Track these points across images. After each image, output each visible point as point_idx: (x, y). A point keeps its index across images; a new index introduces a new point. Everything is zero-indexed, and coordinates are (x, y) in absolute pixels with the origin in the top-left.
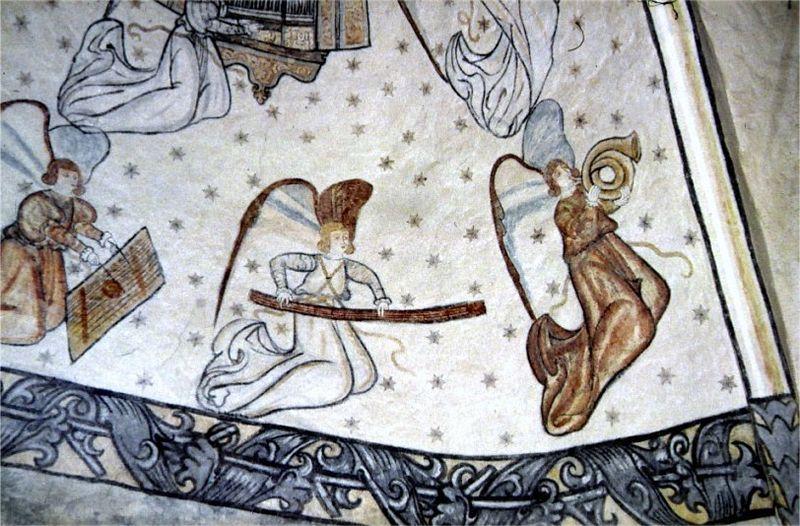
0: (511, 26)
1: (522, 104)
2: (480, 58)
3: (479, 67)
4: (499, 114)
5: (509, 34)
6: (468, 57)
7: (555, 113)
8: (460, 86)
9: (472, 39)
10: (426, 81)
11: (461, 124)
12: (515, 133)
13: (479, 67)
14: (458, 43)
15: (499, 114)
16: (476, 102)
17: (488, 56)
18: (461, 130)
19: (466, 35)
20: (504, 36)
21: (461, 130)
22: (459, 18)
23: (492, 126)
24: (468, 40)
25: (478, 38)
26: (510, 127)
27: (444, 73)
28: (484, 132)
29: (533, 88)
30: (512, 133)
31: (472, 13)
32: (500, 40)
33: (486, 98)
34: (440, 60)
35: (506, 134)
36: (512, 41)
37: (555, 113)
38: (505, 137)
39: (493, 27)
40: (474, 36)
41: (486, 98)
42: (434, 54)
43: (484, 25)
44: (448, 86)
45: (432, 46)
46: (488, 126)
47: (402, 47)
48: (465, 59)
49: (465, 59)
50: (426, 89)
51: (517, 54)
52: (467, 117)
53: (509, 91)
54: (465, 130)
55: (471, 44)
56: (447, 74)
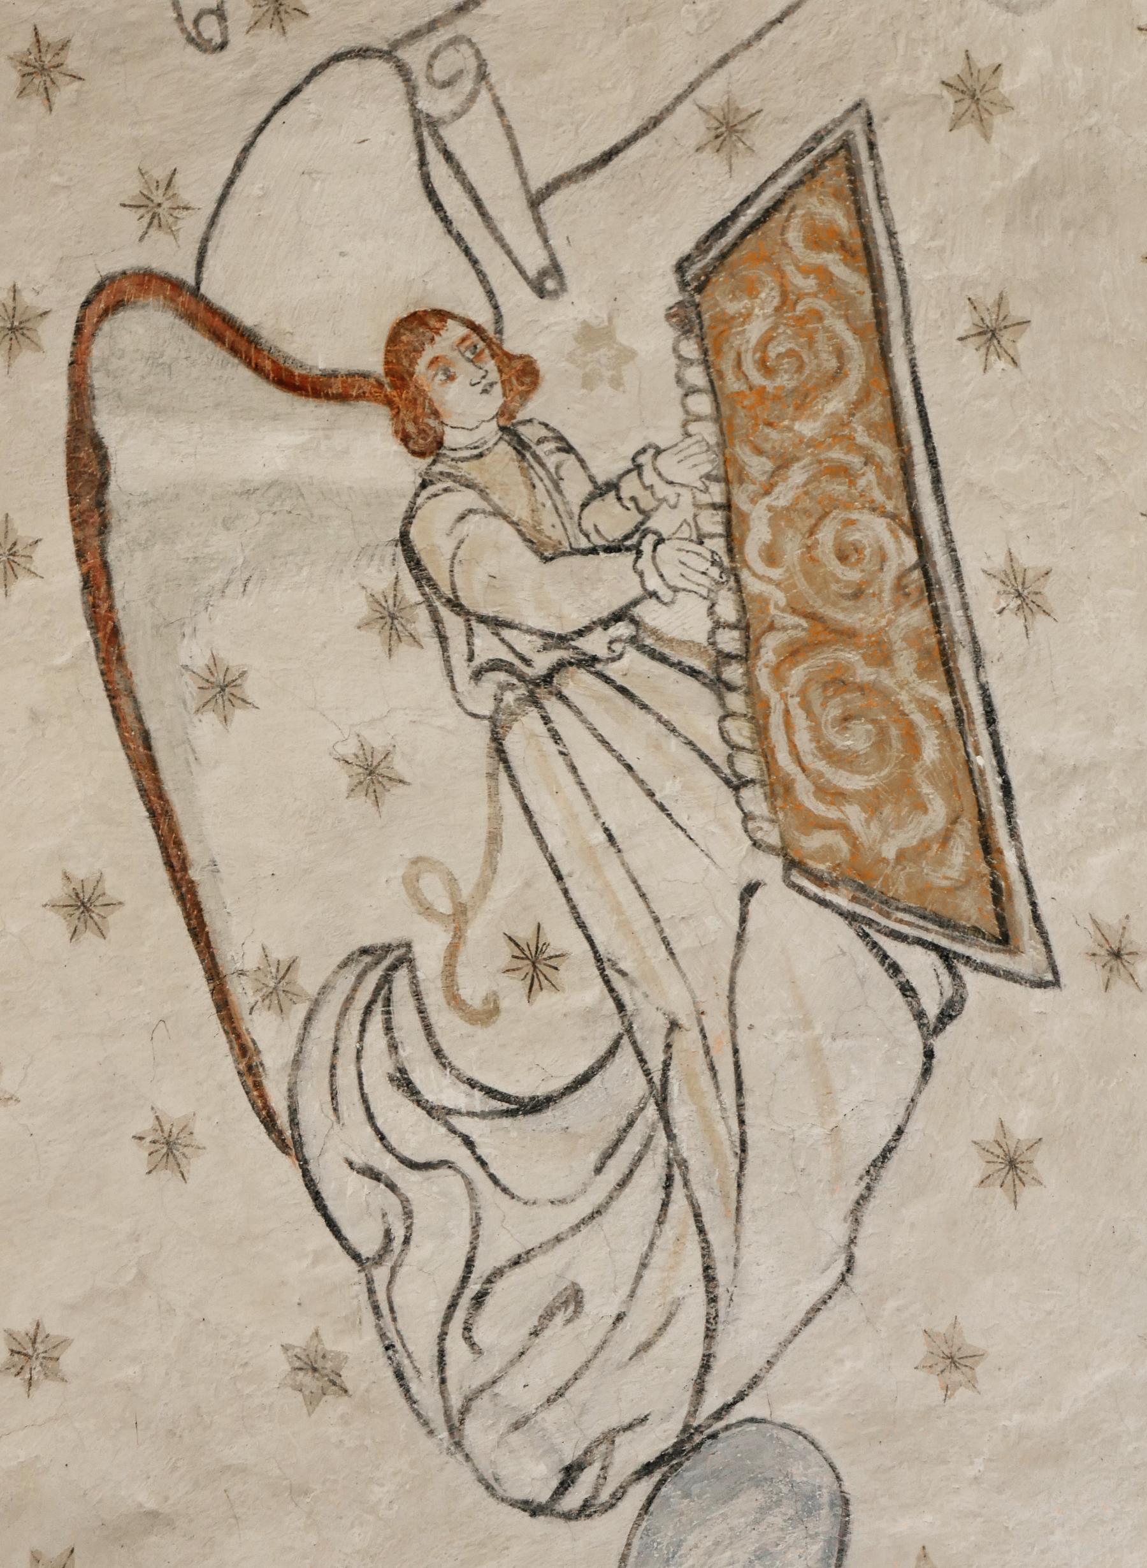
0: (674, 1025)
1: (652, 1398)
2: (479, 1101)
3: (469, 1143)
4: (524, 1389)
5: (655, 1062)
6: (416, 1077)
7: (808, 1505)
8: (348, 1195)
9: (454, 999)
10: (175, 1110)
11: (318, 1374)
12: (585, 1510)
13: (469, 1143)
14: (383, 992)
15: (524, 1389)
16: (421, 1295)
17: (536, 1106)
18: (312, 1401)
19: (429, 965)
20: (626, 1048)
21: (312, 1401)
22: (411, 884)
23: (472, 1429)
24: (434, 999)
25: (489, 1013)
26: (570, 1473)
27: (279, 1103)
28: (432, 1449)
29: (724, 1350)
30: (573, 1500)
31: (483, 888)
32: (601, 1064)
33: (471, 1294)
34: (271, 1035)
35: (544, 1497)
36: (662, 1103)
37: (808, 1505)
38: (533, 1509)
39: (581, 990)
40: (473, 991)
41: (471, 1294)
42: (242, 993)
43: (534, 963)
44: (287, 1166)
45: (239, 948)
46: (454, 1430)
47: (84, 907)
48: (403, 1082)
49: (403, 1082)
50: (168, 1148)
51: (675, 1166)
52: (358, 1348)
53: (600, 1307)
54: (334, 1407)
55: (444, 1020)
56: (293, 1111)
